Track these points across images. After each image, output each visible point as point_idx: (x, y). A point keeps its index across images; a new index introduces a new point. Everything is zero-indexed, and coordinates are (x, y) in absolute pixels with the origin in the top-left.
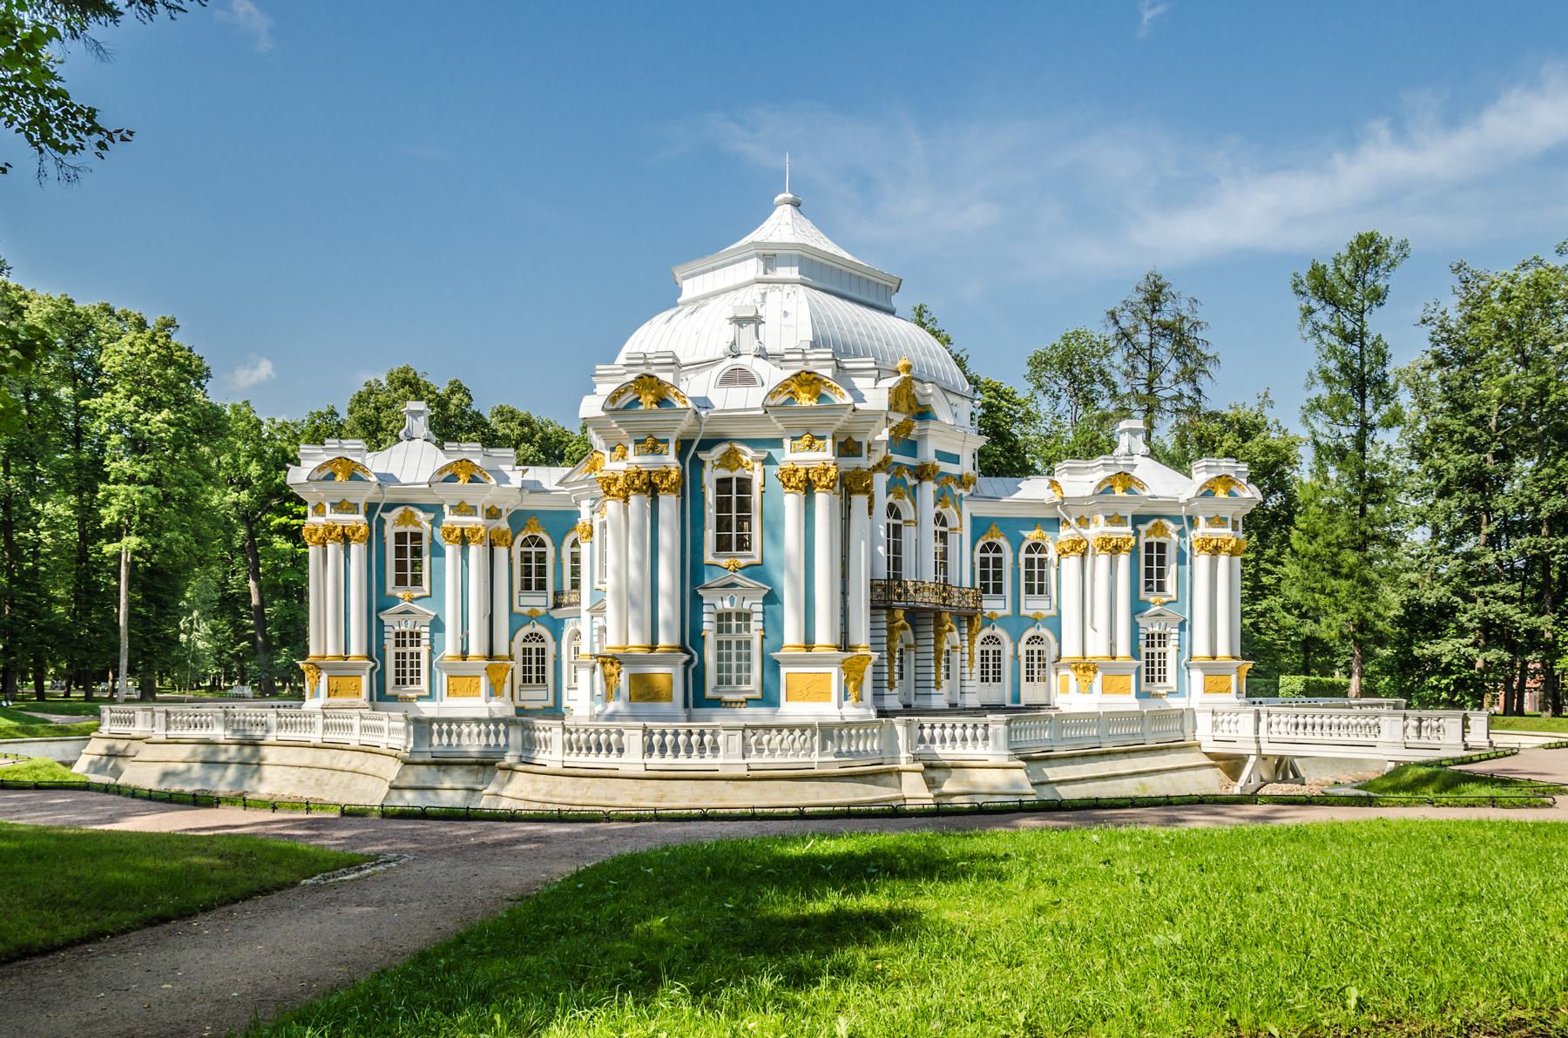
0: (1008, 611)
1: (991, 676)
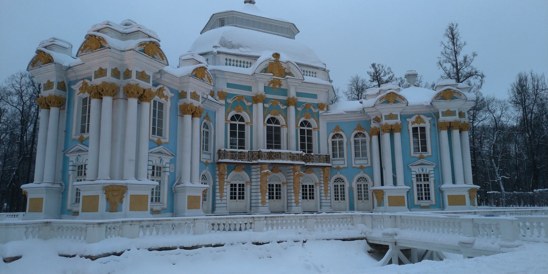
0: (346, 166)
1: (340, 198)
